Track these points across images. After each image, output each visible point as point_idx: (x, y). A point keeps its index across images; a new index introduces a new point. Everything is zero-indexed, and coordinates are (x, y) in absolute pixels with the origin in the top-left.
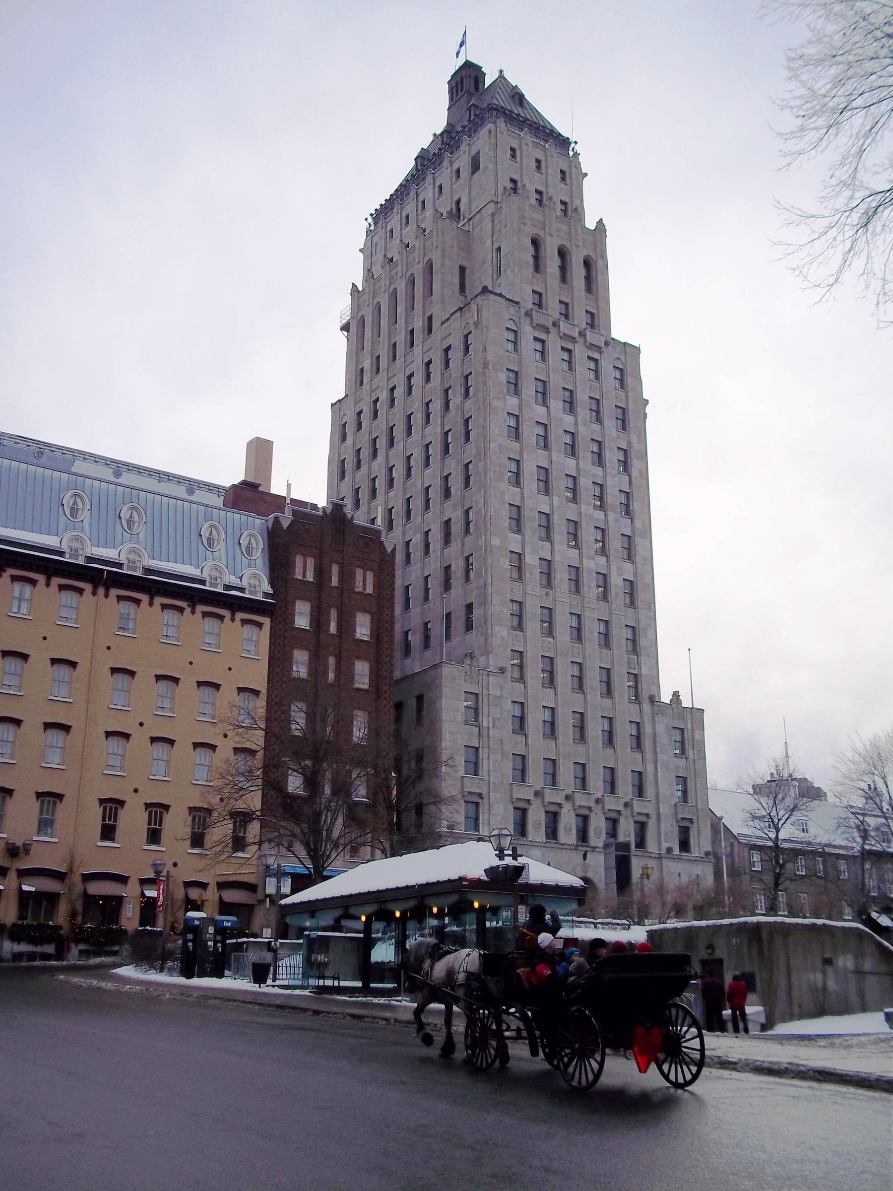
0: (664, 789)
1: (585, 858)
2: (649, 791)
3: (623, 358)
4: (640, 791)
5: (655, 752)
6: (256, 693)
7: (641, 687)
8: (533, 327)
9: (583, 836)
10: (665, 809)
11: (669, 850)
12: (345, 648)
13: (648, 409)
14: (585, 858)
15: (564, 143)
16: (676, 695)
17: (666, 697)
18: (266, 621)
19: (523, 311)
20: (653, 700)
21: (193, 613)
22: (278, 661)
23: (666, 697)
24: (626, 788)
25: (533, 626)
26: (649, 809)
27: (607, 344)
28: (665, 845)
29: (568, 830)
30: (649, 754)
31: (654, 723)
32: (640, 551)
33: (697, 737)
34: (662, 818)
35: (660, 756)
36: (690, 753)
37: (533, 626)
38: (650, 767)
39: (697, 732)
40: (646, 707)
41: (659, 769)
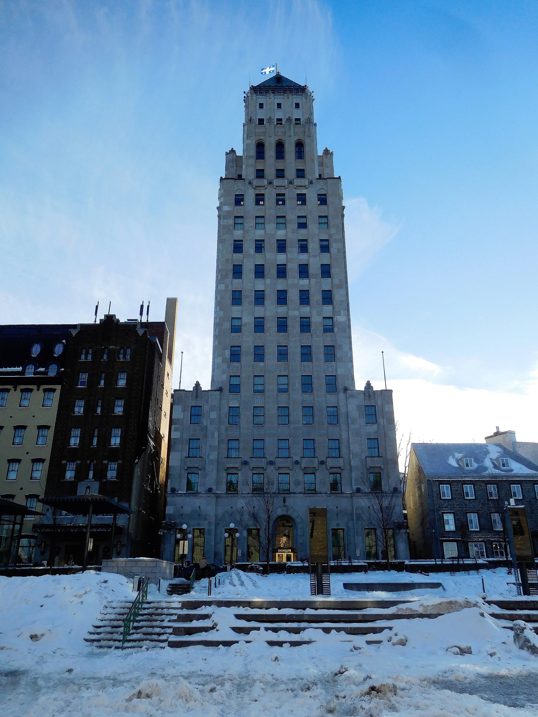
0: (355, 448)
3: (325, 188)
6: (48, 427)
7: (339, 382)
10: (354, 462)
11: (358, 490)
12: (111, 394)
13: (345, 212)
15: (301, 90)
17: (360, 386)
18: (58, 387)
19: (247, 182)
21: (15, 390)
22: (65, 407)
23: (360, 386)
25: (247, 359)
26: (340, 462)
27: (311, 183)
28: (355, 487)
30: (344, 427)
32: (337, 296)
33: (386, 409)
35: (352, 427)
36: (381, 421)
37: (247, 359)
38: (344, 435)
40: (342, 395)
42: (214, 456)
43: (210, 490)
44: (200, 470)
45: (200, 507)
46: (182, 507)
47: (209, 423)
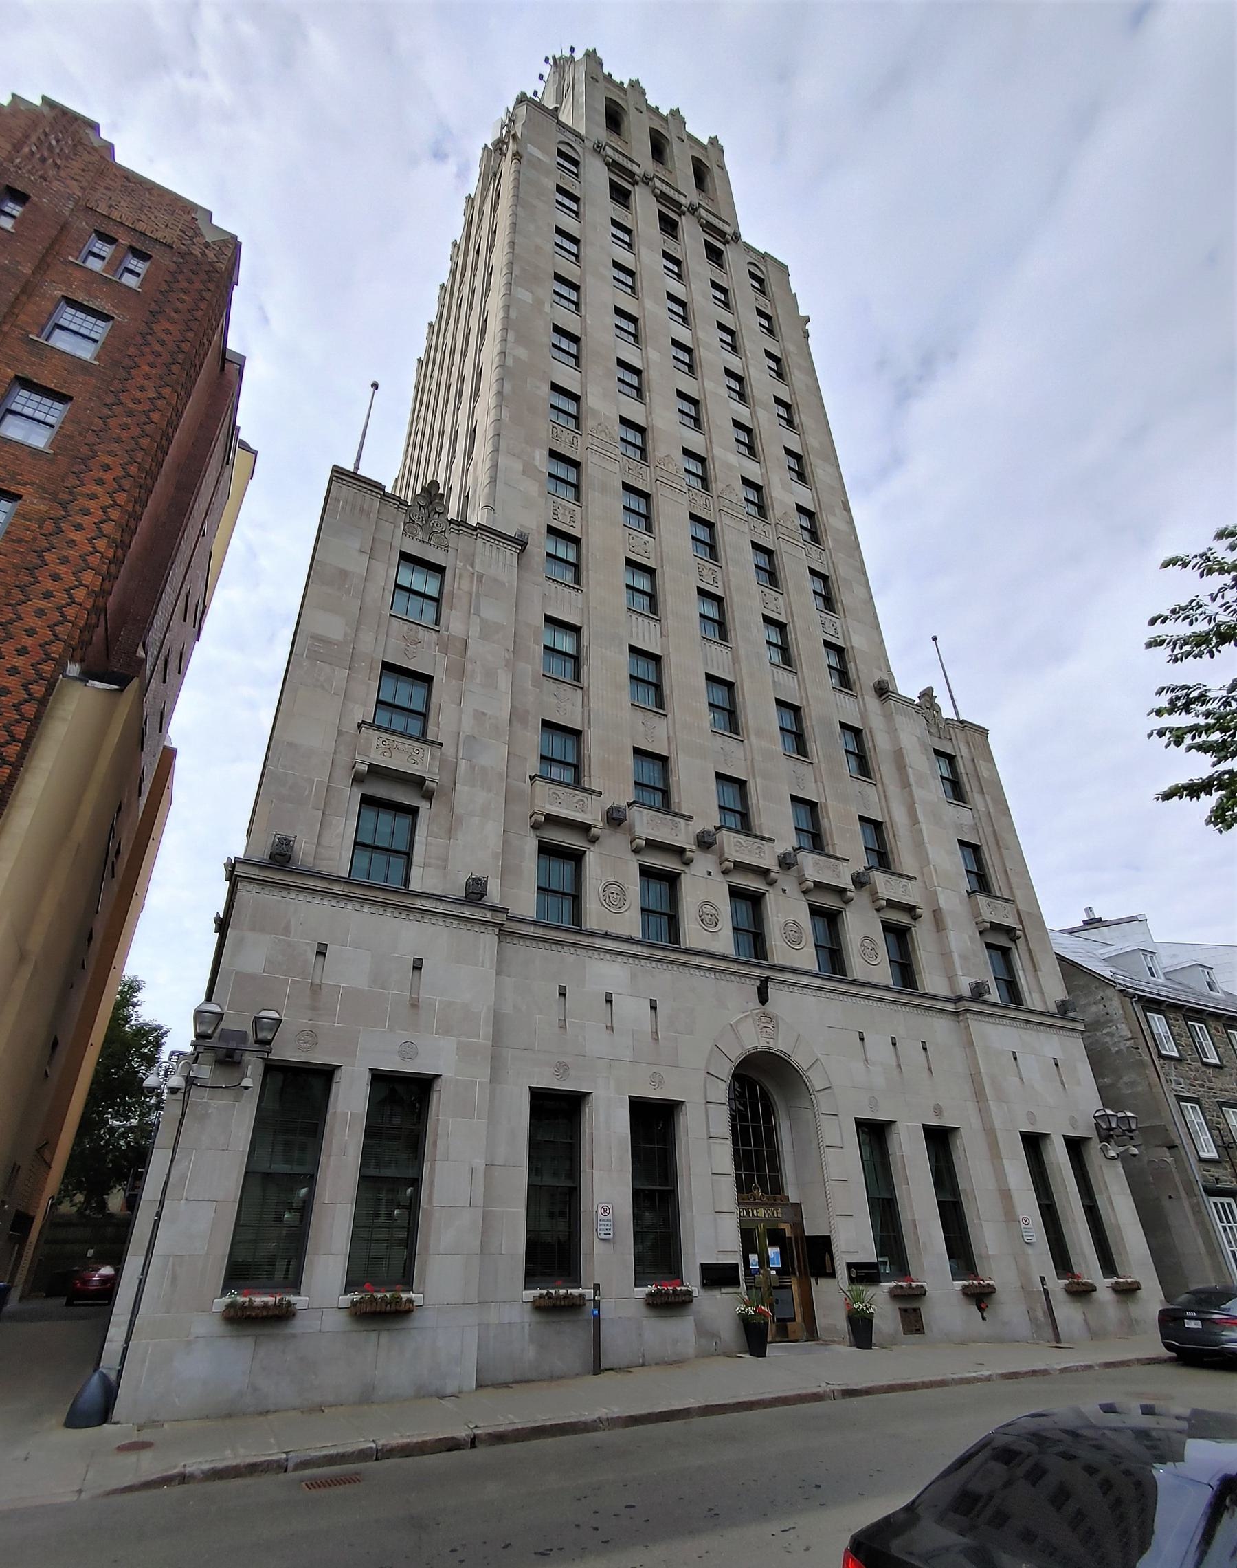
1: (763, 998)
2: (905, 859)
4: (882, 858)
5: (905, 785)
8: (607, 164)
9: (753, 938)
14: (763, 998)
16: (927, 694)
19: (589, 144)
20: (883, 691)
24: (850, 845)
26: (908, 893)
29: (708, 920)
31: (893, 731)
33: (985, 773)
34: (949, 921)
35: (918, 793)
39: (982, 765)
41: (921, 818)
42: (494, 757)
43: (475, 893)
44: (429, 796)
45: (418, 966)
46: (321, 953)
47: (475, 631)
